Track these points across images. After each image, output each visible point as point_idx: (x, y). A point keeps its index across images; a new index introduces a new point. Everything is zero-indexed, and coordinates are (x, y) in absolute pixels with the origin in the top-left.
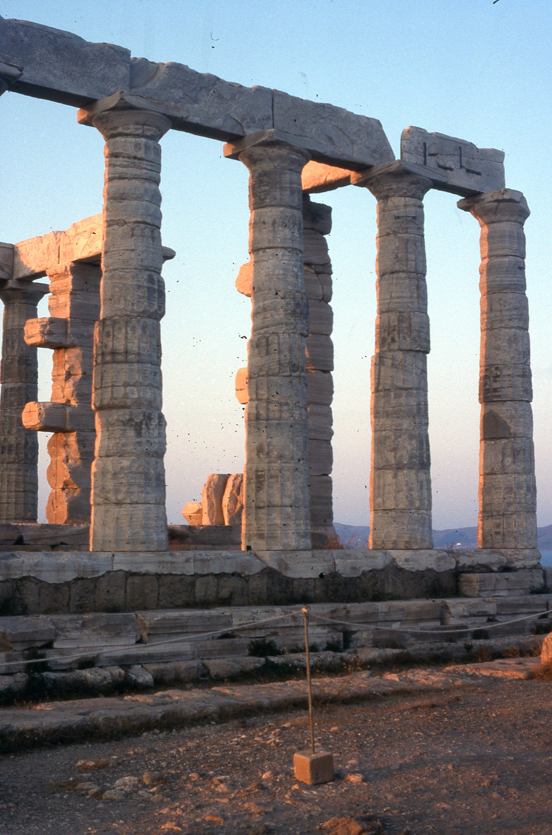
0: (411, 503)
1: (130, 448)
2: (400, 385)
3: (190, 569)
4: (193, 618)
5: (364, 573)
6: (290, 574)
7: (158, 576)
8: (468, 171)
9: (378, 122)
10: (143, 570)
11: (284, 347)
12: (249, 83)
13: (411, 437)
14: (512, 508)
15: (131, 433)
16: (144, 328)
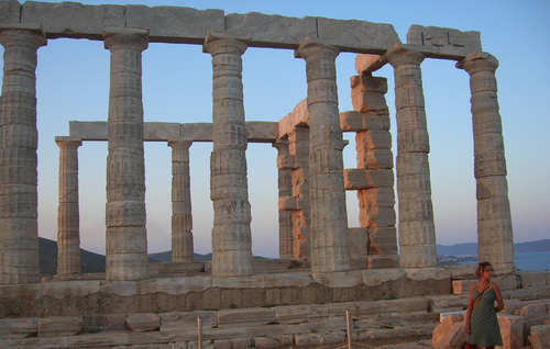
0: (419, 241)
1: (224, 220)
2: (409, 172)
3: (263, 285)
4: (248, 313)
5: (383, 283)
6: (330, 286)
7: (242, 289)
8: (454, 45)
9: (391, 26)
10: (231, 286)
11: (325, 157)
12: (301, 16)
13: (417, 202)
14: (494, 240)
15: (225, 212)
16: (230, 155)
